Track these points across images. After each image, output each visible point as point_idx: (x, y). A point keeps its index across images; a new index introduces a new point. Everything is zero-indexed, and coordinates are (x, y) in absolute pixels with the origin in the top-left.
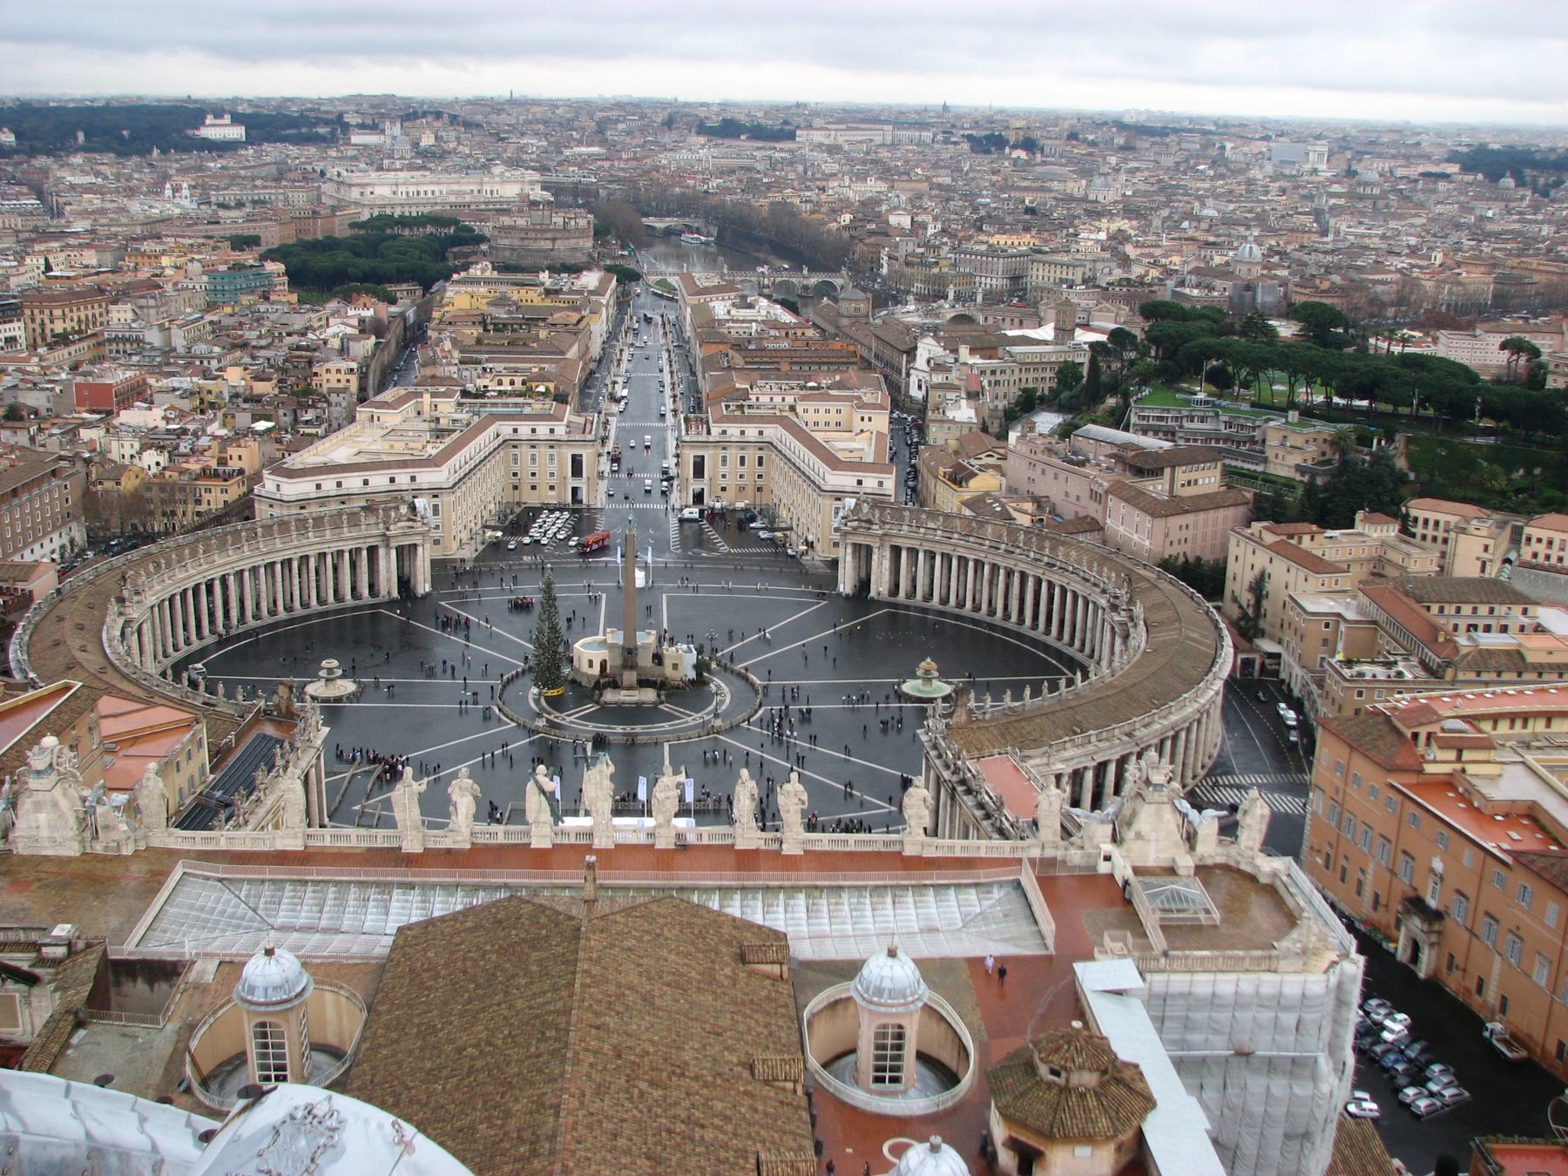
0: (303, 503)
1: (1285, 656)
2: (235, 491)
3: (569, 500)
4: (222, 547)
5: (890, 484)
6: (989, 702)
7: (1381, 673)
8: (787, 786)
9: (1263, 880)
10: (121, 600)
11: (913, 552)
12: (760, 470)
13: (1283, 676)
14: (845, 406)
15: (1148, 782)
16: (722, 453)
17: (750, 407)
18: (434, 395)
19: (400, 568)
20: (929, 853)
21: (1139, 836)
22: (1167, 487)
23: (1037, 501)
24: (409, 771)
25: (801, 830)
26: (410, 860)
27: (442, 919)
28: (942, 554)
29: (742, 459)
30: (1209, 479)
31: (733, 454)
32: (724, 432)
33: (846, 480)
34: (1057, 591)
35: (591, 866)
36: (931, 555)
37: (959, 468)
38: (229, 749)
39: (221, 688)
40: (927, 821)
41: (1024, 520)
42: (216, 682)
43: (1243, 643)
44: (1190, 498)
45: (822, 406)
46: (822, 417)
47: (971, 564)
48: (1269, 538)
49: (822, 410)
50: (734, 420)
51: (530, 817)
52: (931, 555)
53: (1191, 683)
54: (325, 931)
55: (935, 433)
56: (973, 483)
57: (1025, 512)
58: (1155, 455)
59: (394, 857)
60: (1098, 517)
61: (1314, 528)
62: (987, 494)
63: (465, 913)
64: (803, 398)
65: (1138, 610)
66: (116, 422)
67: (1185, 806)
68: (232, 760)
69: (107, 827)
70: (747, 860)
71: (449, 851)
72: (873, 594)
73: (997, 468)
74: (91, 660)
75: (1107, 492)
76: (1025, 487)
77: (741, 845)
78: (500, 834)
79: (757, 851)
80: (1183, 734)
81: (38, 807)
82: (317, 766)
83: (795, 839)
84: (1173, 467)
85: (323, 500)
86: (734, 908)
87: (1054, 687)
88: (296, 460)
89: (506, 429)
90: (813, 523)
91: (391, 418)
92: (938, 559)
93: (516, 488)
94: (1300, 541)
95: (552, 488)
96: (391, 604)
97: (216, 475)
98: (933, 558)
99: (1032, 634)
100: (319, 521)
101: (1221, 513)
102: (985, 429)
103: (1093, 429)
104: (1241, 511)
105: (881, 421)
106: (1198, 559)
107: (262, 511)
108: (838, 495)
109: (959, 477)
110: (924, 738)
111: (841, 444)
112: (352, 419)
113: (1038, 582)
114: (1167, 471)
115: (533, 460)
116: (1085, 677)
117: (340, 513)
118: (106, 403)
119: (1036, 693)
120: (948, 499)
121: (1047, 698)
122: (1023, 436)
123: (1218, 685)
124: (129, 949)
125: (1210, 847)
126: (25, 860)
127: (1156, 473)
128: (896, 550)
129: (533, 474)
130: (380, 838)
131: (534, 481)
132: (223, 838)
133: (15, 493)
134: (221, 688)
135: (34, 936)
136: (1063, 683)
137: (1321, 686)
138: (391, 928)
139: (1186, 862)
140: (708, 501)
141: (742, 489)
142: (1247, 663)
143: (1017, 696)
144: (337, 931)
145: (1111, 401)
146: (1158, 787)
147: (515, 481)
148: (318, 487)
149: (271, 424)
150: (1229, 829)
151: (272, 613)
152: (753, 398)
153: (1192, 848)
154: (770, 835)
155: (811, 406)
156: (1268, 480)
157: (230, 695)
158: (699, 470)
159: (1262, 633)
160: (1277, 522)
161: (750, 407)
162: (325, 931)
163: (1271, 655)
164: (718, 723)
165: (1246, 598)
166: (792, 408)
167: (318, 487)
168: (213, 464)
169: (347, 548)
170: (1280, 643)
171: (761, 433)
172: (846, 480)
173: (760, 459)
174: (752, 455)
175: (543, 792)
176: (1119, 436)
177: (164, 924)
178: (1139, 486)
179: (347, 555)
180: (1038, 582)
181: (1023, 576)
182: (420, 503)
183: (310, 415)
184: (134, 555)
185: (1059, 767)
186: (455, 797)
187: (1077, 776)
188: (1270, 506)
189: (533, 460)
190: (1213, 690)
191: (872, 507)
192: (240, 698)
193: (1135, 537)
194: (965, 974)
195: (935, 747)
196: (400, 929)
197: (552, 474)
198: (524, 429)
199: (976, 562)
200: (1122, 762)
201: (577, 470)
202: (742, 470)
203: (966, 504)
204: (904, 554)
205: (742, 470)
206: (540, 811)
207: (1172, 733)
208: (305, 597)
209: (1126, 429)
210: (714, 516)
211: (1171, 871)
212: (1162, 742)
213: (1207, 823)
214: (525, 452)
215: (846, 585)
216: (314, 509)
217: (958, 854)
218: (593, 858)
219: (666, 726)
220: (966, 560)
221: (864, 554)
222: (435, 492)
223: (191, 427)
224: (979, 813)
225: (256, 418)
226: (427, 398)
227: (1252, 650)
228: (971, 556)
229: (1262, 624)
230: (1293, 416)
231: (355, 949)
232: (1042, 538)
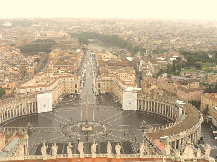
0: (24, 94)
1: (213, 119)
2: (11, 92)
3: (75, 92)
4: (8, 102)
6: (156, 129)
8: (117, 145)
11: (140, 101)
12: (111, 86)
13: (213, 122)
14: (127, 73)
15: (187, 143)
16: (104, 83)
17: (109, 74)
18: (49, 73)
20: (145, 157)
21: (185, 154)
22: (189, 87)
23: (163, 90)
25: (120, 154)
28: (146, 101)
29: (108, 84)
30: (197, 85)
31: (106, 83)
32: (104, 79)
34: (168, 107)
36: (144, 101)
37: (149, 84)
39: (8, 130)
40: (144, 152)
41: (161, 94)
42: (7, 128)
43: (205, 116)
44: (193, 89)
45: (122, 73)
46: (122, 75)
47: (152, 103)
48: (209, 96)
49: (122, 74)
52: (144, 101)
53: (195, 124)
55: (144, 78)
56: (152, 87)
57: (161, 92)
58: (186, 81)
60: (176, 93)
62: (154, 89)
67: (194, 147)
70: (110, 159)
71: (52, 159)
73: (156, 84)
75: (177, 88)
76: (161, 87)
77: (108, 157)
80: (194, 134)
82: (27, 144)
83: (119, 156)
84: (190, 83)
85: (28, 93)
87: (168, 126)
88: (22, 86)
89: (62, 79)
91: (40, 77)
92: (145, 102)
94: (215, 96)
95: (72, 90)
97: (7, 89)
98: (144, 102)
99: (164, 115)
100: (27, 97)
101: (199, 91)
102: (153, 77)
103: (174, 77)
105: (134, 76)
106: (195, 100)
107: (16, 95)
109: (149, 86)
110: (143, 136)
111: (127, 81)
113: (164, 106)
114: (189, 84)
117: (31, 96)
119: (165, 127)
121: (167, 128)
122: (161, 78)
123: (200, 124)
125: (199, 155)
127: (187, 84)
129: (68, 88)
134: (8, 130)
136: (170, 125)
141: (108, 90)
142: (206, 120)
143: (161, 127)
145: (177, 71)
146: (189, 144)
147: (65, 89)
148: (27, 91)
149: (17, 79)
150: (203, 152)
152: (109, 72)
153: (196, 156)
155: (120, 73)
156: (207, 85)
158: (99, 86)
159: (208, 114)
160: (210, 93)
161: (109, 74)
163: (210, 118)
164: (104, 134)
165: (205, 107)
166: (117, 74)
167: (27, 91)
168: (6, 87)
170: (212, 116)
171: (111, 79)
174: (109, 83)
175: (70, 147)
176: (179, 78)
178: (183, 87)
179: (32, 104)
180: (164, 106)
181: (162, 105)
183: (25, 77)
190: (199, 125)
192: (12, 131)
193: (183, 96)
195: (146, 137)
197: (71, 87)
198: (66, 79)
199: (153, 102)
201: (76, 87)
202: (108, 86)
203: (150, 91)
204: (139, 101)
207: (191, 134)
208: (24, 112)
209: (180, 76)
210: (102, 94)
212: (189, 136)
214: (66, 83)
216: (26, 95)
217: (150, 158)
218: (80, 160)
219: (94, 135)
220: (151, 102)
223: (2, 80)
224: (154, 150)
225: (15, 78)
226: (47, 73)
227: (206, 118)
228: (151, 101)
229: (208, 112)
230: (212, 72)
232: (165, 97)
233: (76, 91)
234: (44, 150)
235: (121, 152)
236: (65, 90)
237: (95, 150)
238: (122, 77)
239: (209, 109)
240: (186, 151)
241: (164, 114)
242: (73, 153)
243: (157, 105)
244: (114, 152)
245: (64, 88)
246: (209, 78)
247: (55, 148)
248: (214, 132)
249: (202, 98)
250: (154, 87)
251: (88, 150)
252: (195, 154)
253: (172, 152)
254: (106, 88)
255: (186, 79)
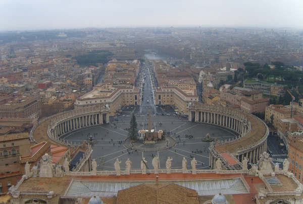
0: (84, 106)
5: (197, 100)
7: (299, 134)
9: (289, 177)
10: (50, 125)
11: (203, 113)
13: (278, 135)
19: (103, 118)
21: (263, 169)
24: (117, 159)
26: (118, 177)
27: (127, 189)
30: (260, 97)
31: (166, 95)
33: (189, 99)
35: (157, 178)
38: (74, 155)
39: (71, 143)
41: (225, 106)
50: (165, 88)
51: (142, 168)
52: (207, 113)
54: (103, 192)
56: (214, 99)
59: (114, 177)
61: (282, 106)
62: (217, 101)
63: (131, 188)
64: (179, 83)
65: (249, 123)
66: (47, 91)
68: (74, 157)
69: (58, 172)
70: (185, 175)
72: (195, 121)
74: (45, 137)
78: (136, 171)
79: (187, 174)
81: (44, 167)
86: (184, 185)
90: (182, 108)
91: (100, 89)
96: (102, 125)
100: (87, 109)
102: (215, 88)
103: (236, 88)
104: (267, 102)
105: (195, 87)
107: (76, 107)
108: (188, 102)
111: (188, 92)
112: (92, 89)
113: (228, 118)
115: (127, 96)
116: (241, 136)
118: (44, 87)
119: (231, 140)
120: (209, 101)
122: (223, 90)
123: (266, 137)
124: (65, 196)
126: (42, 178)
128: (200, 112)
130: (112, 173)
132: (75, 173)
133: (29, 105)
134: (71, 143)
135: (45, 194)
137: (287, 136)
138: (116, 190)
139: (273, 174)
140: (162, 104)
144: (105, 192)
150: (281, 166)
151: (79, 127)
154: (190, 170)
156: (272, 96)
157: (73, 143)
158: (160, 98)
162: (103, 192)
169: (96, 114)
172: (189, 99)
174: (170, 95)
175: (144, 163)
177: (70, 191)
180: (228, 118)
181: (225, 117)
182: (107, 105)
184: (52, 116)
185: (237, 154)
186: (127, 164)
187: (241, 156)
188: (273, 101)
189: (127, 96)
190: (265, 138)
191: (195, 104)
194: (232, 198)
196: (119, 191)
200: (249, 153)
201: (136, 99)
202: (168, 97)
204: (201, 113)
205: (168, 97)
206: (144, 167)
209: (243, 87)
210: (163, 107)
211: (270, 175)
213: (277, 166)
214: (126, 95)
215: (190, 119)
221: (193, 113)
222: (109, 103)
223: (61, 92)
230: (275, 83)
231: (110, 195)
233: (136, 103)
234: (117, 165)
235: (197, 167)
237: (170, 165)
239: (273, 121)
240: (265, 166)
241: (228, 126)
242: (147, 168)
243: (221, 117)
244: (189, 167)
246: (272, 89)
247: (128, 163)
248: (281, 144)
249: (266, 110)
250: (216, 99)
251: (163, 165)
252: (274, 169)
253: (249, 167)
254: (166, 100)
255: (249, 90)
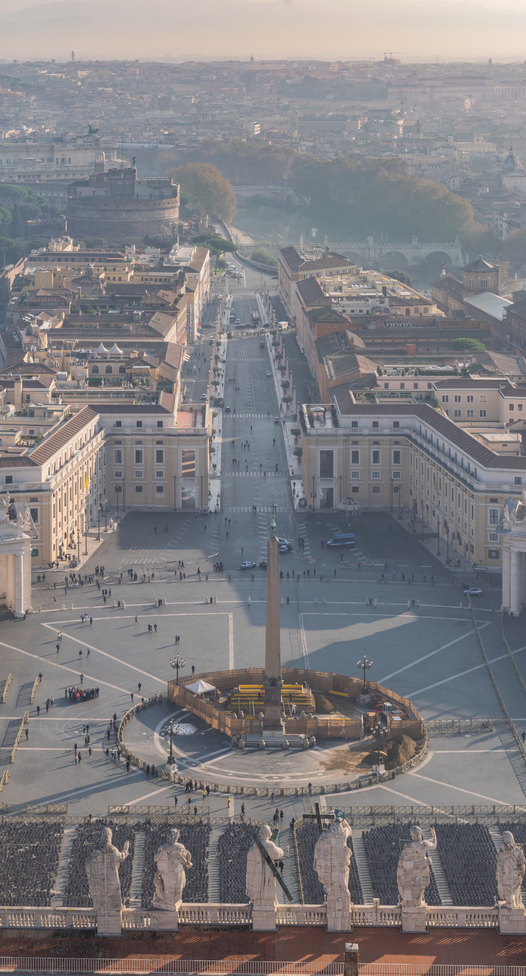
12: (396, 468)
16: (354, 448)
17: (382, 395)
32: (355, 424)
49: (464, 399)
93: (118, 489)
95: (160, 489)
115: (139, 454)
129: (139, 474)
131: (140, 483)
140: (339, 505)
141: (376, 490)
158: (327, 470)
161: (382, 395)
173: (397, 454)
197: (160, 474)
202: (374, 467)
205: (374, 467)
214: (129, 450)
236: (118, 489)
238: (477, 414)
245: (118, 474)
